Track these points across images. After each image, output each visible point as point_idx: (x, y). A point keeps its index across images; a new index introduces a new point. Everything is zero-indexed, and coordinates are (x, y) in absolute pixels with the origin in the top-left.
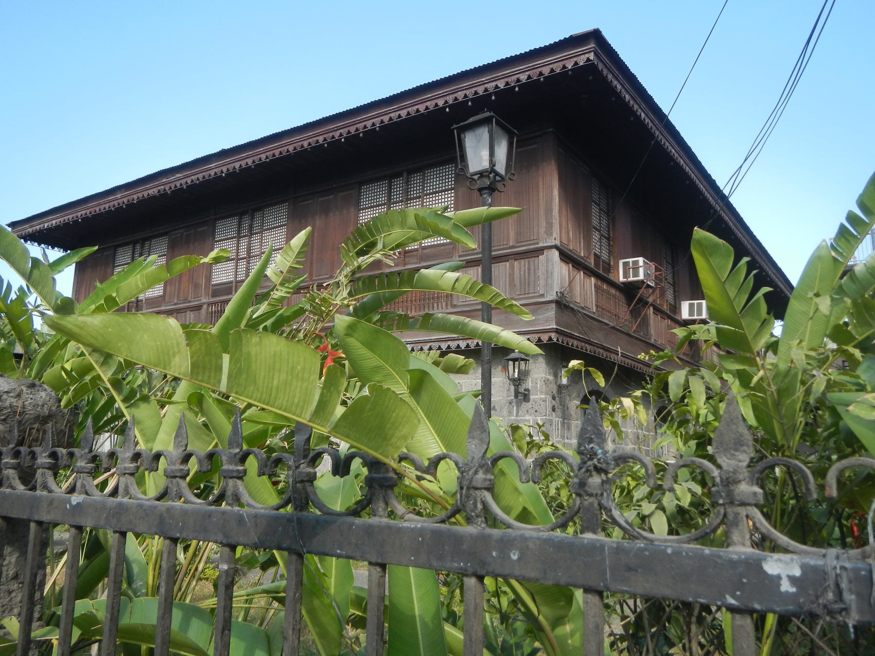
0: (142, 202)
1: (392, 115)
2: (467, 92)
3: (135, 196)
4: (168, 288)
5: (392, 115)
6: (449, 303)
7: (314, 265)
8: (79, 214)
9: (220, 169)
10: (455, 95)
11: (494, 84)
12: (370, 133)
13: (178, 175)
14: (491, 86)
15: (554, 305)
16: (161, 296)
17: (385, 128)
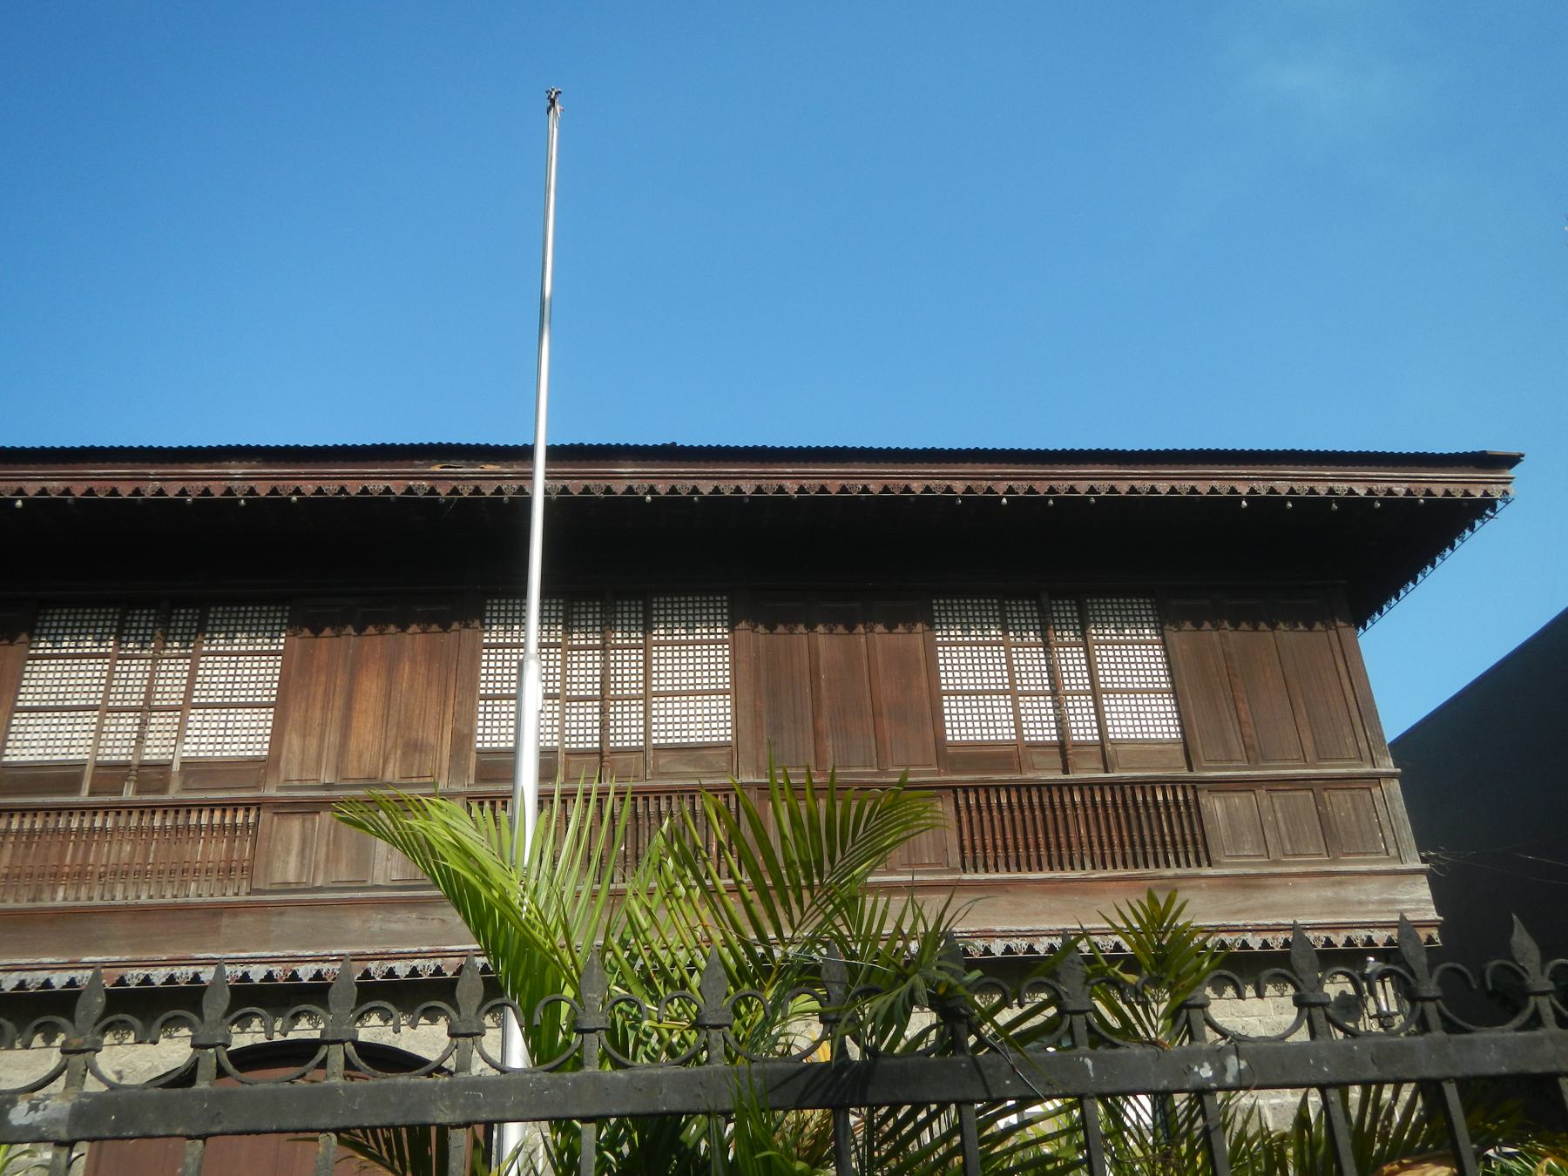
0: (319, 505)
1: (1137, 484)
2: (1296, 486)
3: (307, 484)
4: (293, 741)
5: (1137, 484)
6: (1202, 855)
7: (829, 743)
8: (32, 489)
9: (646, 484)
10: (1271, 484)
11: (1346, 486)
12: (1072, 505)
13: (489, 468)
14: (1341, 488)
15: (1424, 879)
16: (254, 760)
17: (1112, 503)
